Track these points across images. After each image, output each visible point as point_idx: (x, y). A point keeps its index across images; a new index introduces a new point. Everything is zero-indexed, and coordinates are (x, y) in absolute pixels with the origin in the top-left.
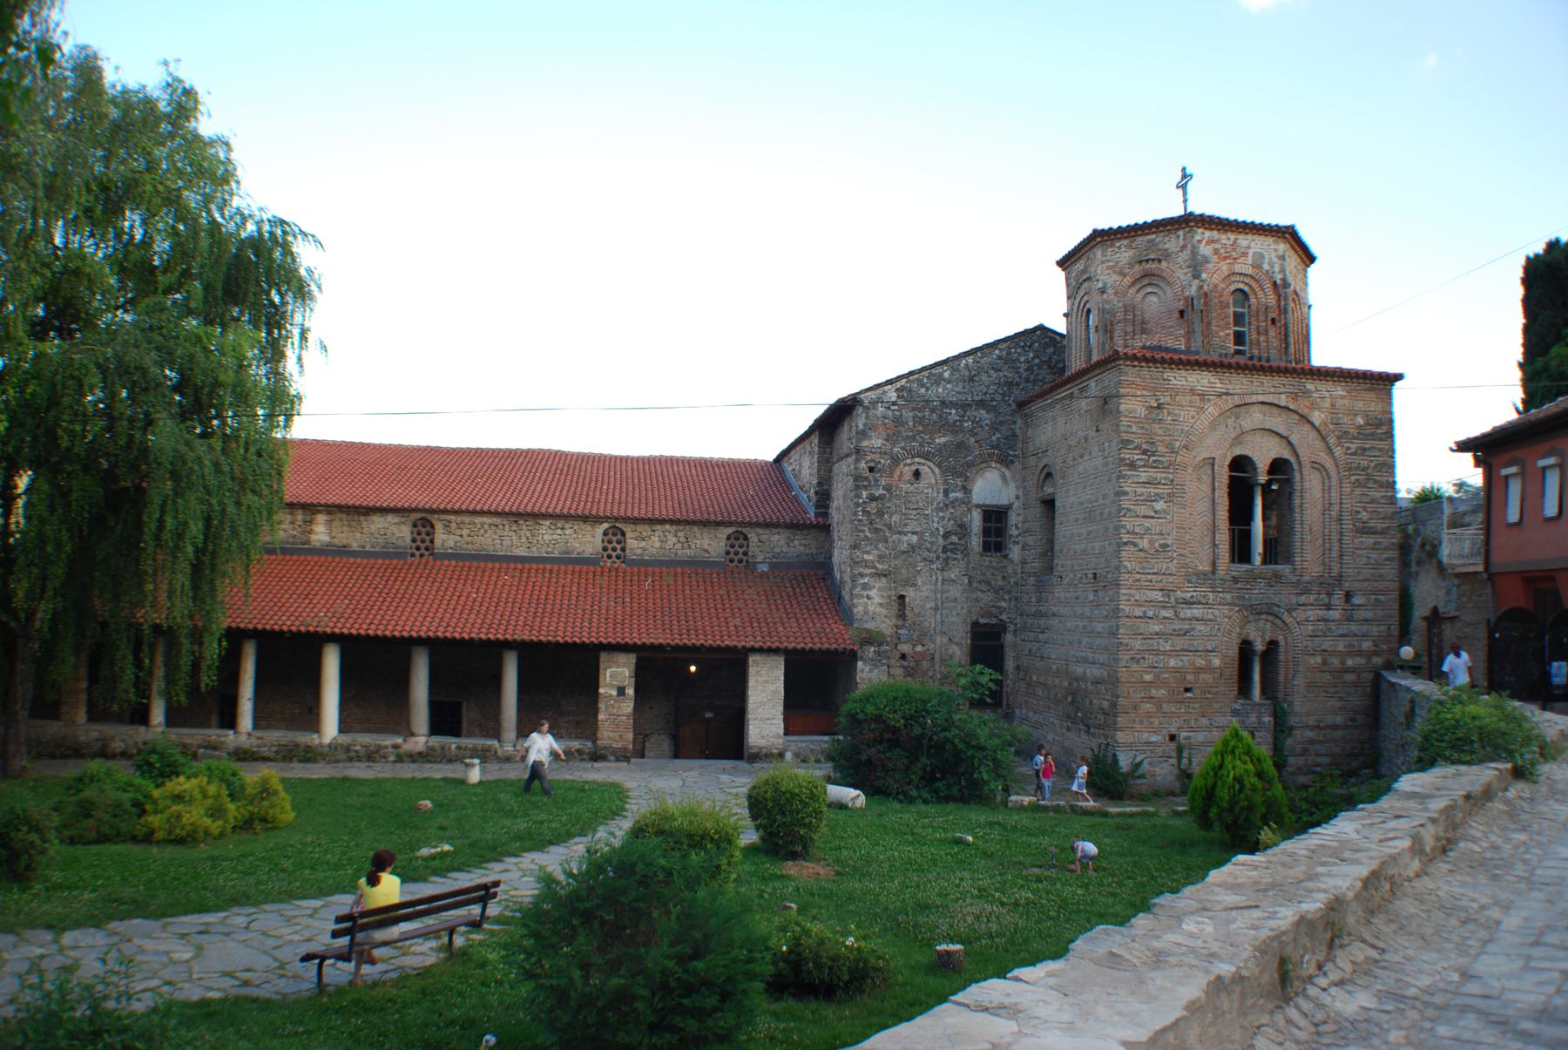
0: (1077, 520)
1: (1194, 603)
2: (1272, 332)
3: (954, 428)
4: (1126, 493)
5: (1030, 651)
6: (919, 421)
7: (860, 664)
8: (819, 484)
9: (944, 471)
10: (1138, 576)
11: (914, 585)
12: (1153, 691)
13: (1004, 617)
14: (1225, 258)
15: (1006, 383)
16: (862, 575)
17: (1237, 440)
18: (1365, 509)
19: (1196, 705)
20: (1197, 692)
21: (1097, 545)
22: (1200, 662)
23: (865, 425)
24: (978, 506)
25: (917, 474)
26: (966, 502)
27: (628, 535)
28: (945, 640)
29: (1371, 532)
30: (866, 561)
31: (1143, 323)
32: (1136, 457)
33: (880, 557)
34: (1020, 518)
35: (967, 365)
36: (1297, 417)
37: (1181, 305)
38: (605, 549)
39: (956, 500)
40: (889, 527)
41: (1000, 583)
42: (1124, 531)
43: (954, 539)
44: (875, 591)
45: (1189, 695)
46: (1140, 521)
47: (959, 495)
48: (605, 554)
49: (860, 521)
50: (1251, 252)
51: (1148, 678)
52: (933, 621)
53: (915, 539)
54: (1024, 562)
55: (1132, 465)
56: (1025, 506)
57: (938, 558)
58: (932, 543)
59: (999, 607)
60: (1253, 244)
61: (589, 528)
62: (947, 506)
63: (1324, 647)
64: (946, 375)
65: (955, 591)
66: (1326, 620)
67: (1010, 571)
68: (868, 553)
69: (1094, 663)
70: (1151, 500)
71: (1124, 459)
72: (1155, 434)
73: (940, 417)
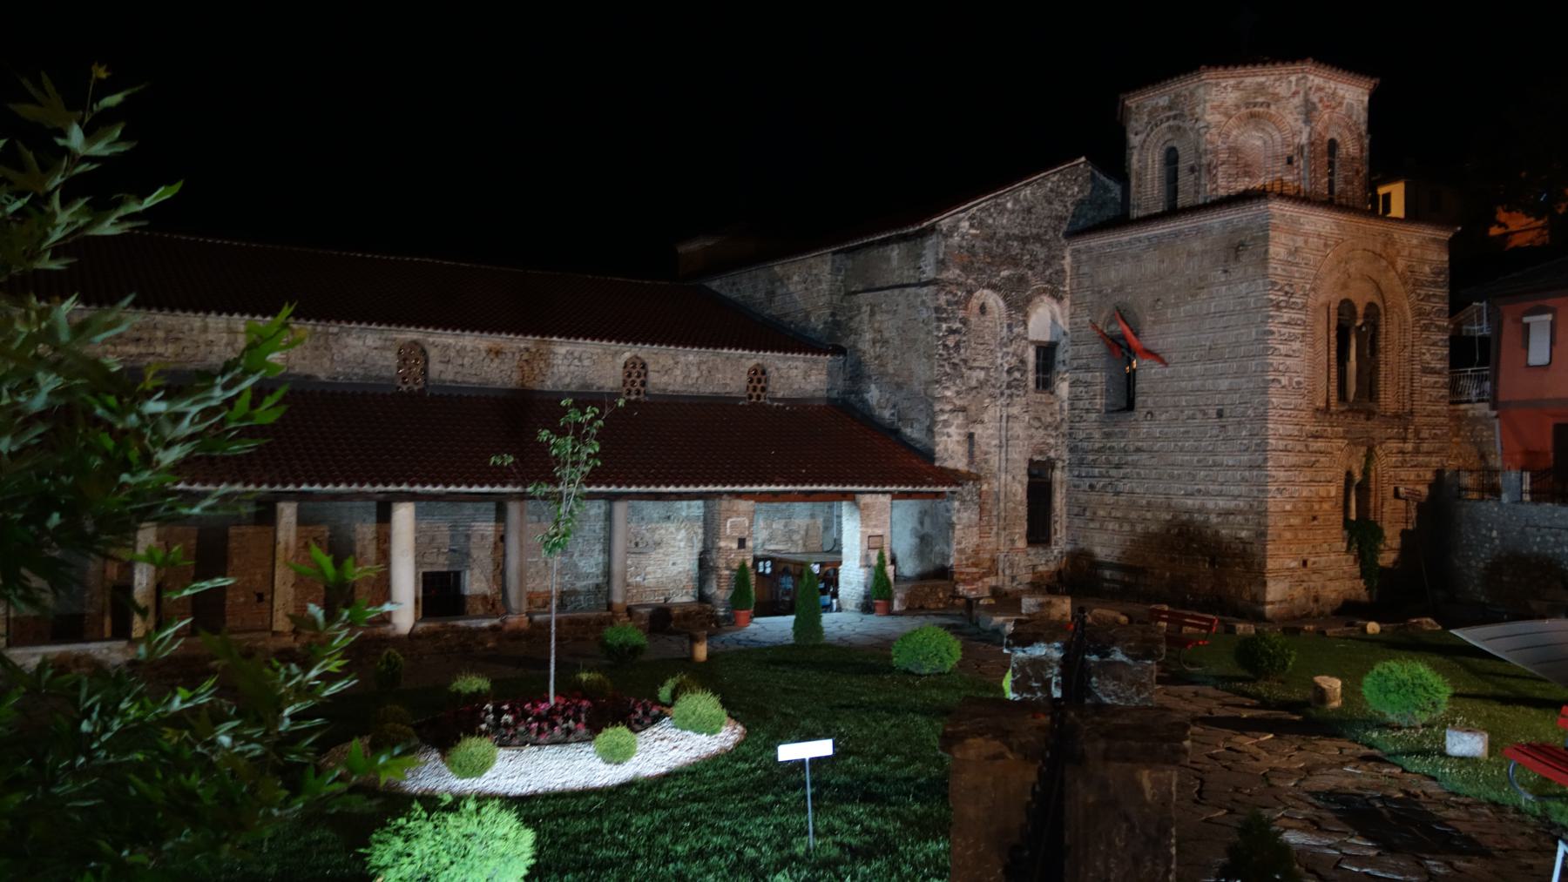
0: (1184, 358)
1: (1317, 437)
2: (1356, 184)
3: (1014, 262)
4: (1272, 333)
5: (1092, 487)
6: (988, 252)
7: (956, 504)
8: (833, 315)
9: (1009, 305)
10: (1282, 412)
11: (982, 422)
12: (1292, 520)
13: (1052, 454)
14: (1327, 107)
15: (1056, 216)
16: (942, 411)
17: (1345, 286)
18: (1429, 350)
19: (1320, 532)
20: (1321, 519)
21: (1224, 384)
22: (1323, 493)
23: (945, 254)
24: (1033, 342)
25: (983, 309)
26: (1026, 339)
27: (651, 367)
28: (1010, 478)
29: (1433, 372)
30: (945, 397)
31: (1246, 165)
32: (1281, 298)
33: (958, 393)
34: (1067, 356)
35: (1025, 195)
36: (1384, 263)
37: (1289, 151)
38: (625, 383)
39: (1018, 335)
40: (965, 361)
41: (1049, 419)
42: (1271, 369)
43: (1017, 375)
44: (953, 428)
45: (1316, 523)
46: (1281, 359)
47: (1020, 330)
48: (624, 390)
49: (941, 355)
50: (1345, 102)
51: (1288, 507)
52: (997, 458)
53: (982, 375)
54: (1074, 398)
55: (1278, 307)
56: (1074, 343)
57: (1002, 394)
58: (996, 379)
59: (1048, 444)
60: (1347, 95)
61: (609, 358)
62: (1011, 341)
63: (1402, 477)
64: (1009, 205)
65: (1018, 429)
66: (1402, 452)
67: (1057, 408)
68: (947, 388)
69: (1220, 494)
70: (1291, 339)
71: (1272, 300)
72: (1294, 277)
73: (1005, 249)
